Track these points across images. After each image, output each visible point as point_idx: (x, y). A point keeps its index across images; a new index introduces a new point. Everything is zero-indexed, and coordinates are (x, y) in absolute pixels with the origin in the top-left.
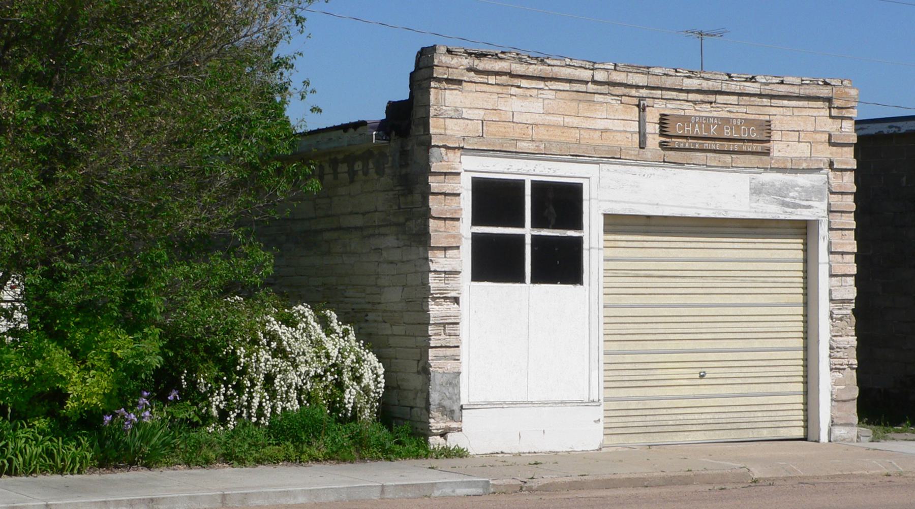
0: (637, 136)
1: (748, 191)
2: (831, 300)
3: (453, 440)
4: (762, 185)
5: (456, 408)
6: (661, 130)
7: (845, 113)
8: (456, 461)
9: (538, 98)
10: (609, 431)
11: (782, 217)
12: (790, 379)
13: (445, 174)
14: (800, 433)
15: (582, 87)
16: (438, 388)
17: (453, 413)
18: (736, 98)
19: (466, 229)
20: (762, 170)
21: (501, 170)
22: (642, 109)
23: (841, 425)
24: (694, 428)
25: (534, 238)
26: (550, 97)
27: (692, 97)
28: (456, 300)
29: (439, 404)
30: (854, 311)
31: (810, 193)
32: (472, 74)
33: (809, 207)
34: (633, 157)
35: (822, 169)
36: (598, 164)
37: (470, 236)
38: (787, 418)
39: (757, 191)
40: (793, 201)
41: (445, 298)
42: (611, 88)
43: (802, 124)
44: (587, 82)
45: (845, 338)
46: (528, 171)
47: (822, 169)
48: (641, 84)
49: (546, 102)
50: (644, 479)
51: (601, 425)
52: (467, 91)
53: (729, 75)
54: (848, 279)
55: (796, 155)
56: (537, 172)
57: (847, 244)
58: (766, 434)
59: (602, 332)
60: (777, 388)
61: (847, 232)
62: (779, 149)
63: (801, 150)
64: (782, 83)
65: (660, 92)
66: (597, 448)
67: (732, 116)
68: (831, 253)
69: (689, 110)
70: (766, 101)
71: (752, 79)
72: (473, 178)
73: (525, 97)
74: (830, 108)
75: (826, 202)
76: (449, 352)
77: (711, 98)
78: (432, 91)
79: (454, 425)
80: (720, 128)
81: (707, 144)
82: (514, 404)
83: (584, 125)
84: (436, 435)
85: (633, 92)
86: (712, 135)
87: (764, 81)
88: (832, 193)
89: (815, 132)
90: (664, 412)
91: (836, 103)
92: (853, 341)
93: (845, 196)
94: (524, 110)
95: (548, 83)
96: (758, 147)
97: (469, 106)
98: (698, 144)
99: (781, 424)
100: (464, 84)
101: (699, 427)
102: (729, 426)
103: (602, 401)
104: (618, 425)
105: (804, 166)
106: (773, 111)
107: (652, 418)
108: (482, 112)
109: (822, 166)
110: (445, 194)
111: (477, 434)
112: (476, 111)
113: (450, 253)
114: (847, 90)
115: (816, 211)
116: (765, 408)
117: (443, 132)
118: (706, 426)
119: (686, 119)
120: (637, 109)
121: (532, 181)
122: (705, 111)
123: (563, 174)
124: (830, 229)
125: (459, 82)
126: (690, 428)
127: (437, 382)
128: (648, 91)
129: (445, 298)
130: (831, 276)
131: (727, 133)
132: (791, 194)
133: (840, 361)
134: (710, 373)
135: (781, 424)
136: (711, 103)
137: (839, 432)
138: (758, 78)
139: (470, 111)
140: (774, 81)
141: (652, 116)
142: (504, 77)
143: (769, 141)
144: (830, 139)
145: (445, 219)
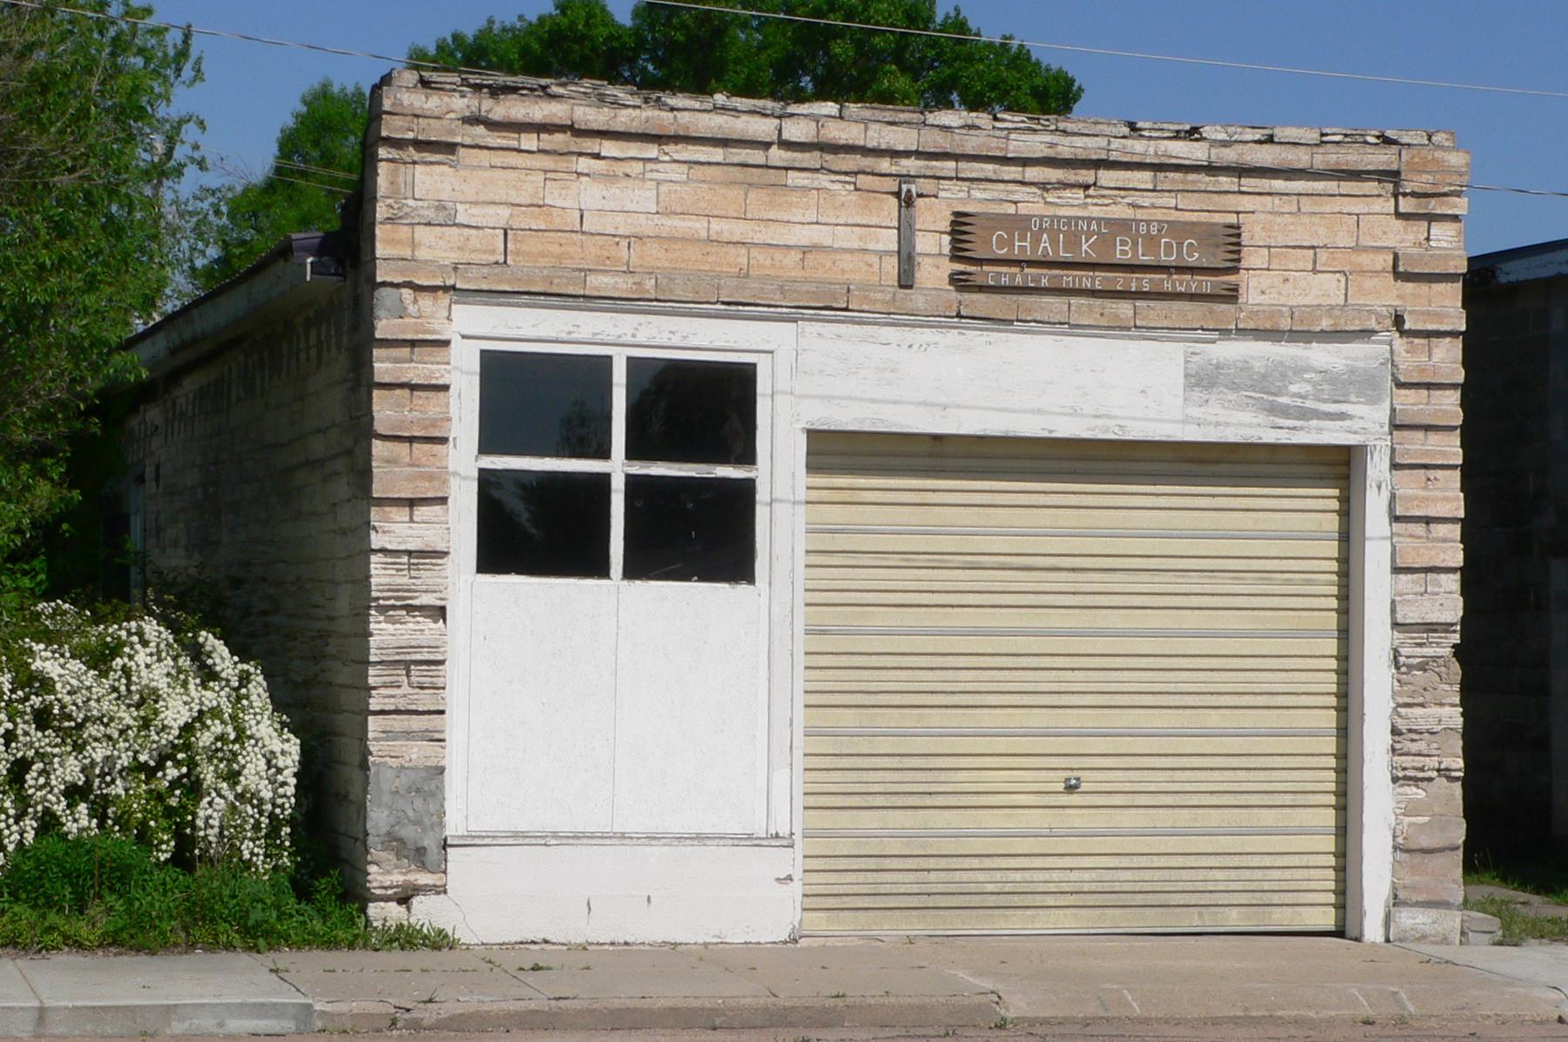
0: (895, 260)
1: (1181, 380)
2: (1396, 625)
3: (426, 913)
4: (1218, 367)
5: (430, 842)
6: (954, 249)
7: (1435, 206)
8: (423, 957)
9: (644, 180)
10: (814, 901)
11: (1270, 437)
12: (1300, 799)
13: (413, 344)
14: (1327, 919)
15: (756, 156)
16: (386, 798)
17: (427, 853)
18: (1148, 175)
19: (463, 462)
20: (1215, 335)
21: (553, 335)
22: (907, 202)
23: (1418, 904)
25: (632, 482)
26: (675, 177)
27: (1032, 173)
28: (440, 613)
29: (389, 834)
30: (1459, 651)
31: (1342, 386)
32: (481, 129)
33: (1342, 416)
34: (879, 307)
35: (1374, 332)
36: (795, 321)
37: (476, 474)
38: (1293, 886)
39: (1202, 380)
40: (1299, 402)
41: (410, 609)
42: (828, 157)
43: (1322, 231)
44: (767, 145)
45: (1435, 710)
47: (1374, 332)
48: (901, 148)
49: (664, 188)
50: (714, 1011)
51: (796, 888)
53: (1132, 127)
54: (1443, 577)
55: (1309, 300)
56: (641, 339)
57: (1436, 500)
58: (1235, 919)
59: (800, 687)
60: (1268, 818)
61: (1439, 473)
62: (1260, 289)
63: (1324, 290)
64: (1270, 140)
66: (785, 937)
67: (1140, 214)
68: (1396, 519)
69: (1031, 204)
70: (1225, 182)
71: (1193, 134)
72: (482, 352)
73: (611, 178)
74: (1396, 196)
75: (1386, 405)
77: (1087, 176)
78: (383, 168)
79: (424, 879)
80: (1106, 241)
81: (1069, 278)
83: (760, 238)
84: (387, 899)
85: (885, 165)
86: (1082, 258)
87: (1222, 136)
88: (1400, 385)
89: (1357, 249)
90: (975, 863)
92: (1453, 716)
93: (1436, 393)
94: (608, 205)
96: (1206, 284)
97: (474, 199)
98: (1045, 277)
99: (1276, 898)
100: (462, 151)
103: (798, 838)
104: (856, 889)
105: (1326, 324)
106: (1246, 203)
107: (943, 876)
108: (505, 212)
109: (1372, 324)
110: (413, 387)
111: (478, 902)
112: (491, 210)
113: (421, 512)
114: (1438, 154)
115: (1363, 423)
116: (1236, 861)
117: (407, 253)
118: (1080, 898)
119: (1019, 223)
120: (894, 201)
121: (629, 359)
122: (1070, 205)
123: (706, 344)
124: (1395, 466)
125: (450, 148)
127: (385, 786)
128: (922, 163)
129: (410, 609)
130: (1397, 570)
132: (1293, 388)
133: (1419, 761)
134: (1089, 781)
135: (1276, 898)
136: (1087, 187)
137: (1409, 919)
138: (1207, 131)
139: (474, 210)
140: (1249, 137)
141: (933, 219)
142: (559, 137)
143: (1235, 270)
144: (1395, 265)
145: (411, 440)
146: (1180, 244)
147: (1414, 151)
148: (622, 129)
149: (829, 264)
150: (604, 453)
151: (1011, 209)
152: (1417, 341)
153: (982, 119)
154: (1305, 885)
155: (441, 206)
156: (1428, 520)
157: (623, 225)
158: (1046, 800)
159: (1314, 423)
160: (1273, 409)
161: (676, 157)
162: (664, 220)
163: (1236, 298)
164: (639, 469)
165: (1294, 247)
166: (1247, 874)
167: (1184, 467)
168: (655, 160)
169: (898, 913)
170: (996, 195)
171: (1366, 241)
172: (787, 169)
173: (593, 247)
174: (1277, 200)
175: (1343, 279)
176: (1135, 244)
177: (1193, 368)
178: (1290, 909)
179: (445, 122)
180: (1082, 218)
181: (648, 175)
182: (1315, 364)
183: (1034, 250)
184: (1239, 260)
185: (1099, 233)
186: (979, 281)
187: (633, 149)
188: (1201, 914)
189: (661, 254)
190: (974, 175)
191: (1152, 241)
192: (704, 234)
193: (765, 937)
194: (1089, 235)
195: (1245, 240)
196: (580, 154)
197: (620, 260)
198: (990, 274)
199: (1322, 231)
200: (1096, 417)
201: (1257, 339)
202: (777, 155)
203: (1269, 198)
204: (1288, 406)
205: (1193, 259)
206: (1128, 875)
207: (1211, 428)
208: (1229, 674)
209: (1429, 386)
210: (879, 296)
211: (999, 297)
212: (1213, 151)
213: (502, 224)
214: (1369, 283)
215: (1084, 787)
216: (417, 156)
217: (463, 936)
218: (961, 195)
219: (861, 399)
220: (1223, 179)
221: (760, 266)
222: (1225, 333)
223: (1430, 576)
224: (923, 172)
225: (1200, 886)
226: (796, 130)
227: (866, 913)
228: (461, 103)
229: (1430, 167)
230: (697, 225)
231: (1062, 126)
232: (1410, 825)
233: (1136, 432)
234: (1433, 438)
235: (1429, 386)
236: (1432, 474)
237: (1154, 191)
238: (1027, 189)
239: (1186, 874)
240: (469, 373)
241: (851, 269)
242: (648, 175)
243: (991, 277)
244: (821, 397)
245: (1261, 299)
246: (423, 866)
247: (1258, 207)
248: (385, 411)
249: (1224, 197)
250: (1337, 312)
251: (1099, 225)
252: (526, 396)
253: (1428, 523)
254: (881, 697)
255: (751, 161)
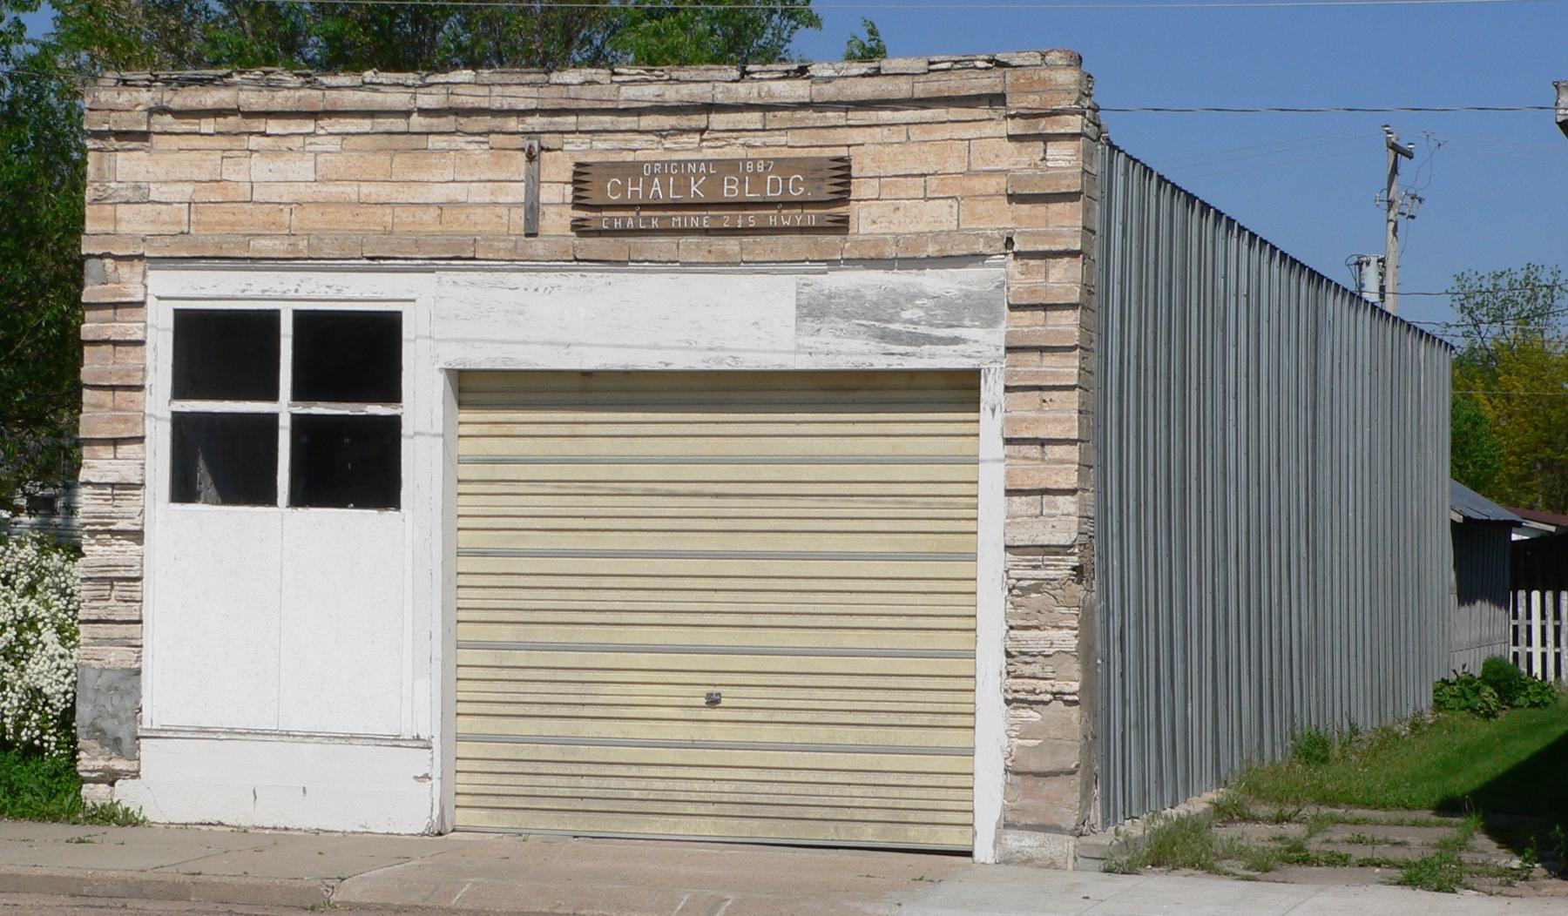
0: (521, 212)
1: (793, 311)
3: (126, 794)
4: (830, 297)
5: (123, 733)
6: (576, 198)
7: (1046, 126)
8: (113, 831)
9: (304, 152)
11: (881, 363)
12: (938, 720)
13: (115, 306)
15: (399, 124)
18: (757, 116)
19: (159, 404)
20: (824, 266)
21: (229, 293)
22: (531, 157)
24: (691, 809)
25: (297, 420)
26: (329, 148)
27: (647, 122)
28: (137, 536)
29: (92, 725)
31: (954, 311)
32: (168, 118)
33: (956, 341)
34: (502, 255)
36: (433, 271)
37: (169, 416)
39: (813, 311)
40: (911, 328)
42: (463, 120)
43: (931, 158)
44: (407, 114)
46: (287, 293)
49: (320, 159)
50: (83, 881)
52: (163, 152)
54: (1060, 499)
55: (919, 228)
56: (302, 294)
58: (868, 835)
61: (1055, 395)
63: (936, 217)
64: (877, 73)
65: (572, 119)
67: (752, 154)
69: (648, 150)
70: (832, 117)
71: (802, 72)
72: (176, 311)
73: (276, 152)
76: (118, 631)
77: (699, 120)
79: (120, 765)
80: (714, 181)
82: (232, 733)
83: (402, 198)
84: (96, 781)
85: (512, 124)
87: (830, 73)
89: (970, 173)
90: (623, 771)
91: (1016, 103)
95: (325, 122)
96: (812, 216)
98: (655, 219)
99: (912, 817)
100: (155, 138)
101: (703, 809)
102: (775, 812)
104: (513, 791)
105: (931, 250)
106: (856, 136)
107: (594, 782)
108: (188, 188)
109: (980, 247)
110: (116, 343)
111: (167, 789)
112: (179, 187)
113: (124, 450)
114: (1045, 74)
115: (979, 346)
116: (872, 778)
117: (110, 229)
118: (720, 808)
121: (295, 312)
122: (686, 148)
123: (357, 296)
125: (144, 136)
126: (681, 808)
128: (545, 120)
130: (1010, 493)
131: (730, 191)
132: (906, 315)
133: (1029, 684)
135: (912, 817)
136: (702, 131)
138: (815, 70)
139: (164, 188)
140: (855, 71)
141: (557, 168)
142: (232, 119)
143: (846, 202)
145: (113, 388)
146: (786, 180)
147: (1019, 72)
148: (278, 109)
149: (463, 218)
150: (273, 396)
151: (629, 157)
152: (1032, 262)
153: (602, 75)
154: (942, 805)
155: (137, 187)
156: (1043, 443)
157: (285, 193)
158: (693, 714)
159: (927, 348)
160: (885, 336)
161: (331, 130)
162: (320, 187)
163: (847, 229)
164: (301, 409)
165: (905, 176)
166: (883, 792)
167: (822, 395)
168: (314, 134)
169: (552, 814)
170: (616, 145)
171: (978, 166)
172: (428, 134)
173: (260, 214)
174: (885, 130)
175: (955, 205)
176: (742, 182)
177: (804, 299)
178: (926, 828)
179: (134, 114)
180: (692, 161)
181: (308, 148)
182: (929, 290)
183: (646, 194)
184: (849, 192)
185: (708, 175)
186: (593, 225)
187: (293, 126)
188: (836, 829)
189: (318, 217)
190: (593, 128)
191: (758, 178)
192: (354, 197)
193: (405, 829)
194: (698, 176)
195: (854, 173)
196: (251, 134)
197: (282, 225)
198: (603, 219)
199: (931, 158)
200: (710, 349)
201: (868, 268)
202: (417, 122)
203: (878, 130)
204: (899, 333)
205: (796, 194)
206: (767, 788)
207: (823, 357)
208: (871, 596)
209: (1045, 307)
210: (502, 245)
211: (612, 240)
212: (814, 87)
213: (187, 199)
214: (981, 207)
215: (724, 702)
216: (117, 145)
217: (151, 814)
218: (584, 147)
219: (492, 341)
220: (829, 114)
221: (403, 223)
222: (833, 263)
223: (1046, 498)
224: (547, 128)
225: (836, 801)
226: (427, 100)
227: (522, 813)
228: (146, 97)
229: (1037, 87)
230: (349, 190)
231: (675, 75)
232: (1020, 747)
233: (750, 362)
234: (1050, 360)
235: (1045, 307)
236: (1047, 395)
237: (764, 130)
238: (645, 137)
239: (822, 790)
240: (164, 330)
241: (483, 221)
242: (308, 148)
243: (615, 221)
244: (456, 340)
245: (876, 228)
246: (121, 755)
247: (867, 139)
248: (93, 365)
249: (833, 131)
250: (943, 238)
251: (707, 167)
252: (220, 348)
253: (1043, 445)
254: (706, 616)
255: (394, 129)
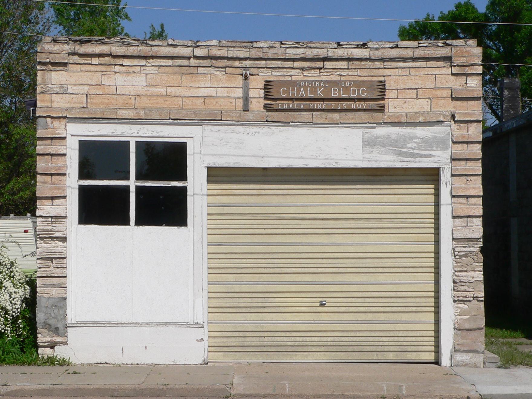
0: (241, 100)
1: (361, 144)
2: (454, 239)
3: (60, 352)
5: (60, 325)
6: (265, 95)
7: (468, 70)
8: (58, 369)
9: (140, 73)
10: (213, 348)
11: (399, 165)
12: (419, 309)
13: (52, 139)
14: (431, 357)
15: (185, 62)
16: (43, 309)
17: (60, 330)
19: (72, 183)
20: (375, 125)
21: (106, 134)
22: (246, 78)
23: (464, 351)
24: (314, 349)
26: (152, 72)
27: (297, 64)
28: (64, 239)
29: (45, 322)
30: (483, 250)
31: (430, 144)
32: (76, 57)
34: (234, 119)
35: (442, 122)
36: (201, 125)
37: (78, 187)
38: (416, 344)
40: (411, 151)
41: (52, 238)
42: (214, 62)
43: (420, 82)
44: (189, 58)
45: (473, 273)
46: (133, 134)
47: (442, 122)
48: (242, 57)
49: (148, 76)
50: (114, 390)
51: (206, 343)
52: (74, 72)
53: (339, 44)
54: (475, 220)
56: (141, 134)
57: (470, 188)
58: (391, 357)
59: (206, 266)
60: (406, 316)
61: (472, 178)
62: (393, 106)
63: (421, 106)
65: (264, 62)
66: (200, 362)
67: (343, 79)
68: (453, 197)
69: (297, 76)
70: (378, 64)
71: (364, 45)
73: (128, 73)
74: (451, 66)
75: (449, 151)
76: (55, 281)
77: (320, 64)
78: (39, 74)
79: (58, 339)
80: (327, 90)
81: (312, 105)
85: (237, 63)
86: (318, 96)
87: (377, 46)
88: (454, 143)
89: (435, 88)
90: (283, 334)
91: (456, 62)
92: (479, 276)
93: (471, 146)
94: (126, 84)
95: (151, 61)
96: (371, 105)
97: (75, 83)
99: (409, 349)
100: (70, 66)
101: (319, 349)
102: (351, 349)
103: (205, 325)
105: (421, 119)
106: (387, 72)
107: (270, 339)
108: (86, 88)
109: (441, 119)
110: (52, 155)
111: (80, 348)
112: (81, 87)
113: (56, 202)
114: (468, 49)
115: (439, 158)
116: (391, 334)
117: (49, 105)
118: (327, 348)
119: (292, 84)
120: (241, 77)
121: (136, 142)
123: (166, 135)
124: (453, 175)
125: (65, 65)
126: (310, 349)
127: (43, 305)
128: (251, 62)
129: (52, 238)
130: (454, 217)
131: (334, 94)
132: (409, 145)
133: (464, 294)
134: (329, 302)
136: (320, 69)
137: (459, 357)
138: (370, 45)
139: (75, 88)
140: (388, 46)
142: (107, 59)
143: (383, 99)
144: (452, 95)
145: (52, 175)
146: (359, 90)
149: (215, 103)
150: (127, 178)
151: (289, 79)
152: (462, 125)
154: (421, 343)
156: (467, 197)
159: (418, 159)
160: (400, 154)
162: (148, 88)
163: (384, 110)
166: (397, 339)
168: (145, 66)
169: (252, 353)
170: (282, 73)
171: (437, 86)
172: (198, 67)
173: (121, 100)
174: (400, 70)
175: (430, 101)
176: (340, 90)
178: (415, 353)
179: (62, 55)
180: (318, 81)
181: (142, 72)
182: (418, 135)
184: (385, 95)
185: (324, 87)
186: (275, 107)
187: (136, 62)
188: (377, 355)
190: (273, 66)
191: (347, 89)
192: (164, 93)
193: (192, 363)
196: (116, 65)
197: (132, 104)
198: (279, 104)
199: (420, 82)
200: (325, 159)
202: (193, 62)
203: (397, 70)
204: (407, 153)
205: (364, 95)
206: (347, 339)
207: (374, 162)
209: (467, 143)
210: (234, 114)
211: (283, 113)
212: (371, 52)
213: (86, 92)
214: (441, 102)
216: (52, 68)
217: (73, 360)
218: (268, 74)
219: (229, 155)
220: (376, 63)
222: (379, 124)
223: (469, 219)
224: (252, 66)
225: (377, 344)
228: (67, 48)
230: (162, 90)
232: (460, 319)
235: (467, 143)
236: (469, 178)
238: (296, 71)
239: (370, 339)
241: (223, 105)
242: (142, 72)
243: (281, 105)
245: (394, 110)
246: (58, 335)
247: (392, 74)
248: (41, 164)
251: (324, 84)
252: (97, 158)
255: (183, 65)
